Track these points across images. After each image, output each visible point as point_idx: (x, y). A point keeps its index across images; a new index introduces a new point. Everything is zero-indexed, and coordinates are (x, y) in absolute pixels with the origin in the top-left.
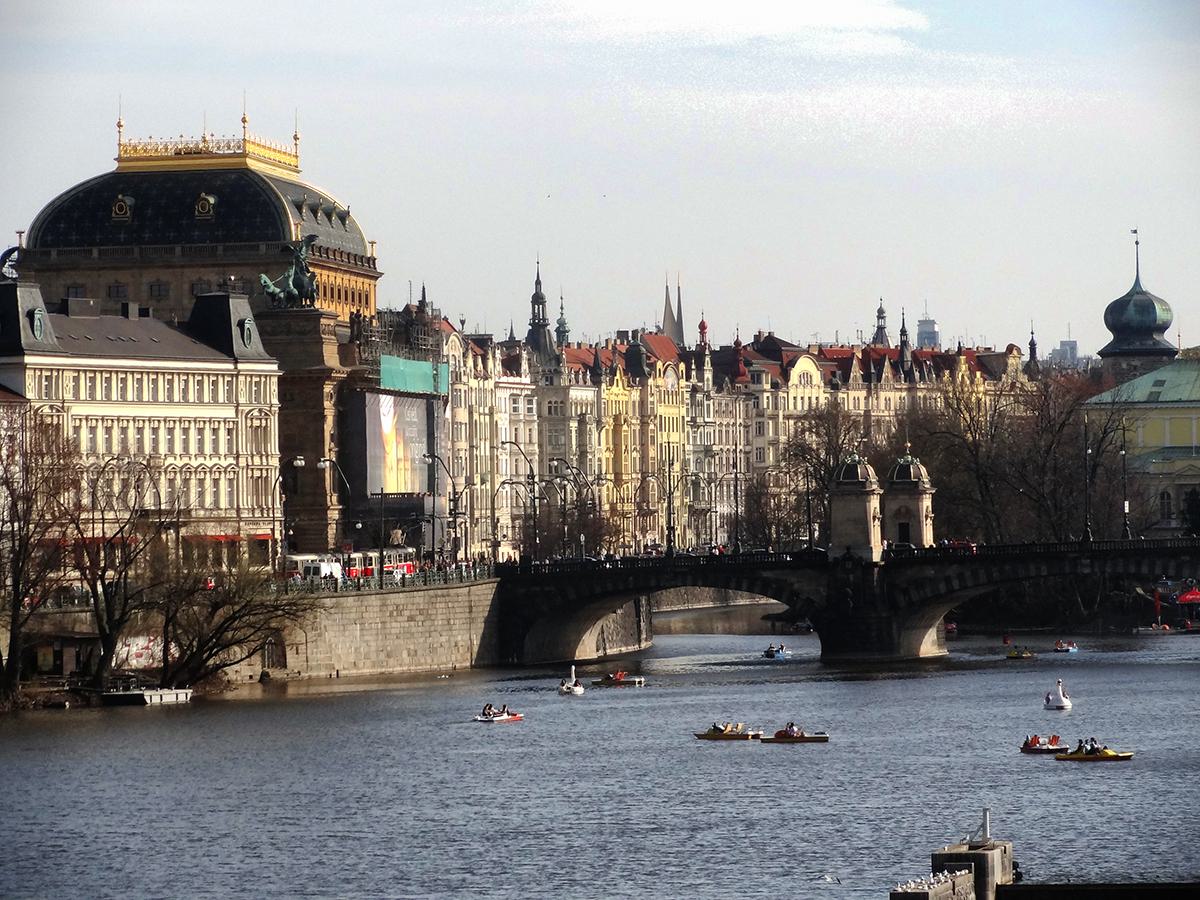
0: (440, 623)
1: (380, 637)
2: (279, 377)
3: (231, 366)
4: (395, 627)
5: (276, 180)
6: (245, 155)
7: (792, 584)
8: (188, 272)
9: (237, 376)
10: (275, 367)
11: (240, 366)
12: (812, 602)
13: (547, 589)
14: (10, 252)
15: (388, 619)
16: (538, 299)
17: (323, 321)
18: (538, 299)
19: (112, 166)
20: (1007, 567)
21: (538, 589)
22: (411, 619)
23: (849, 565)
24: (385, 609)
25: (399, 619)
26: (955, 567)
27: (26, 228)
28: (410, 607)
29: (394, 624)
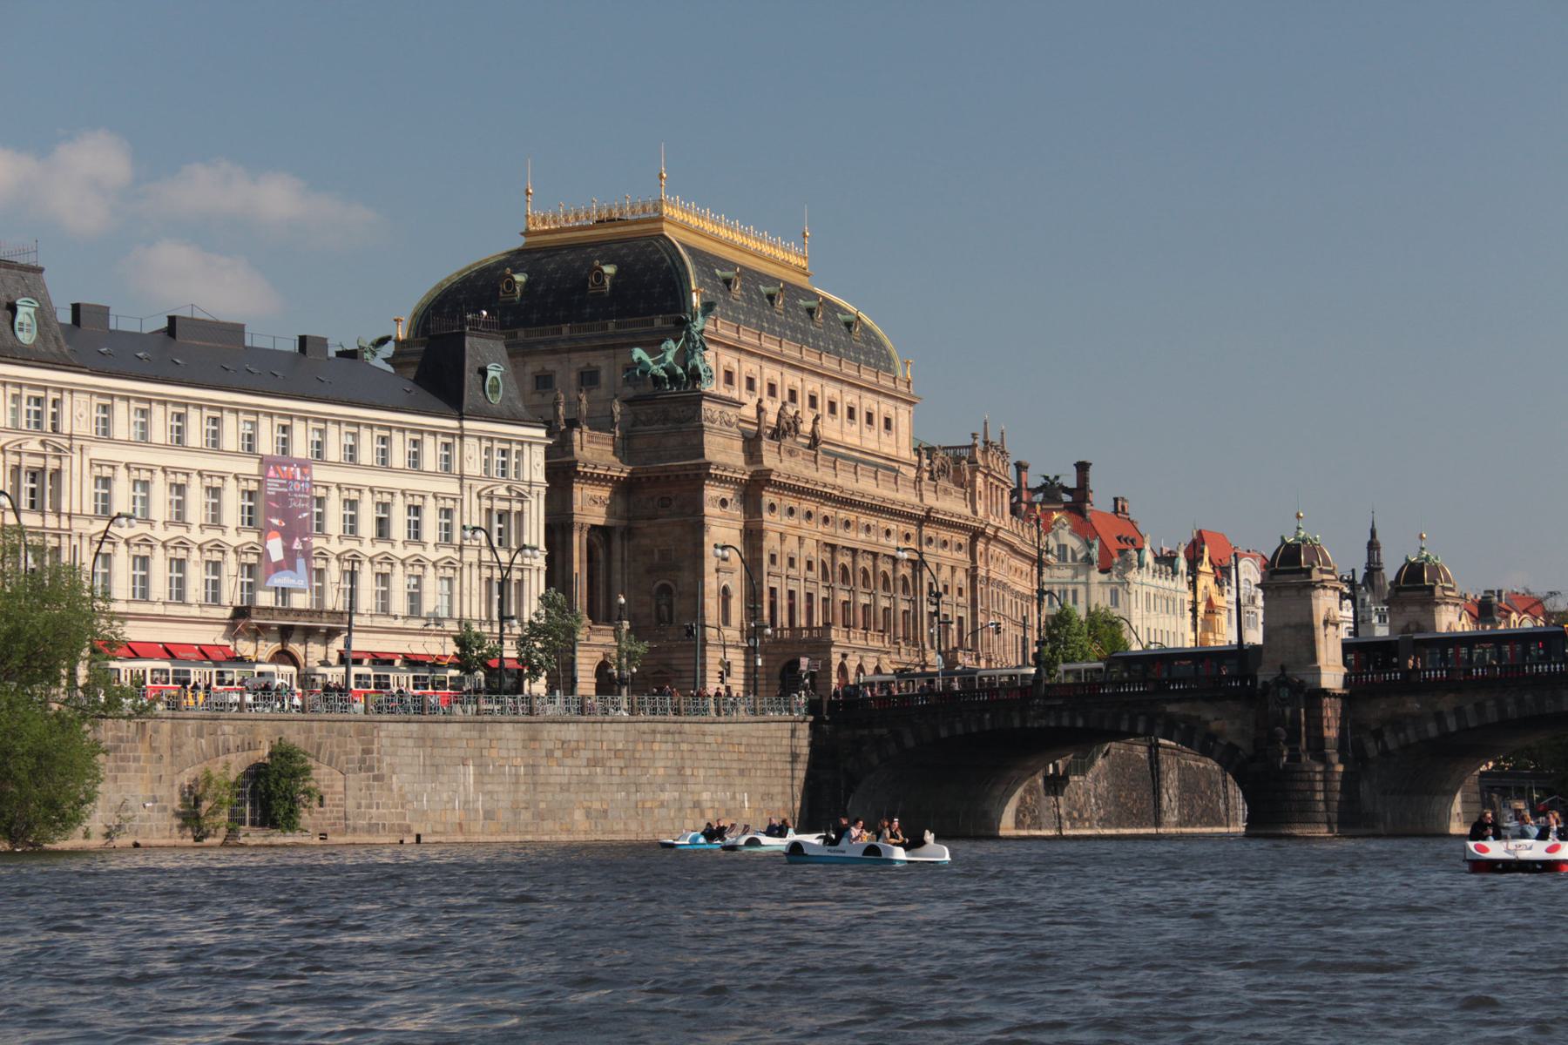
0: (661, 771)
1: (523, 788)
2: (548, 448)
3: (454, 424)
4: (559, 773)
5: (691, 250)
6: (661, 219)
7: (1207, 723)
8: (575, 357)
9: (461, 437)
10: (542, 433)
11: (467, 424)
12: (1237, 749)
13: (877, 731)
14: (383, 341)
15: (544, 762)
16: (1373, 546)
17: (705, 405)
18: (1373, 546)
19: (518, 243)
20: (1528, 697)
21: (866, 732)
22: (593, 762)
23: (1285, 693)
24: (537, 745)
25: (569, 762)
26: (1450, 697)
27: (406, 318)
28: (592, 745)
29: (555, 769)
